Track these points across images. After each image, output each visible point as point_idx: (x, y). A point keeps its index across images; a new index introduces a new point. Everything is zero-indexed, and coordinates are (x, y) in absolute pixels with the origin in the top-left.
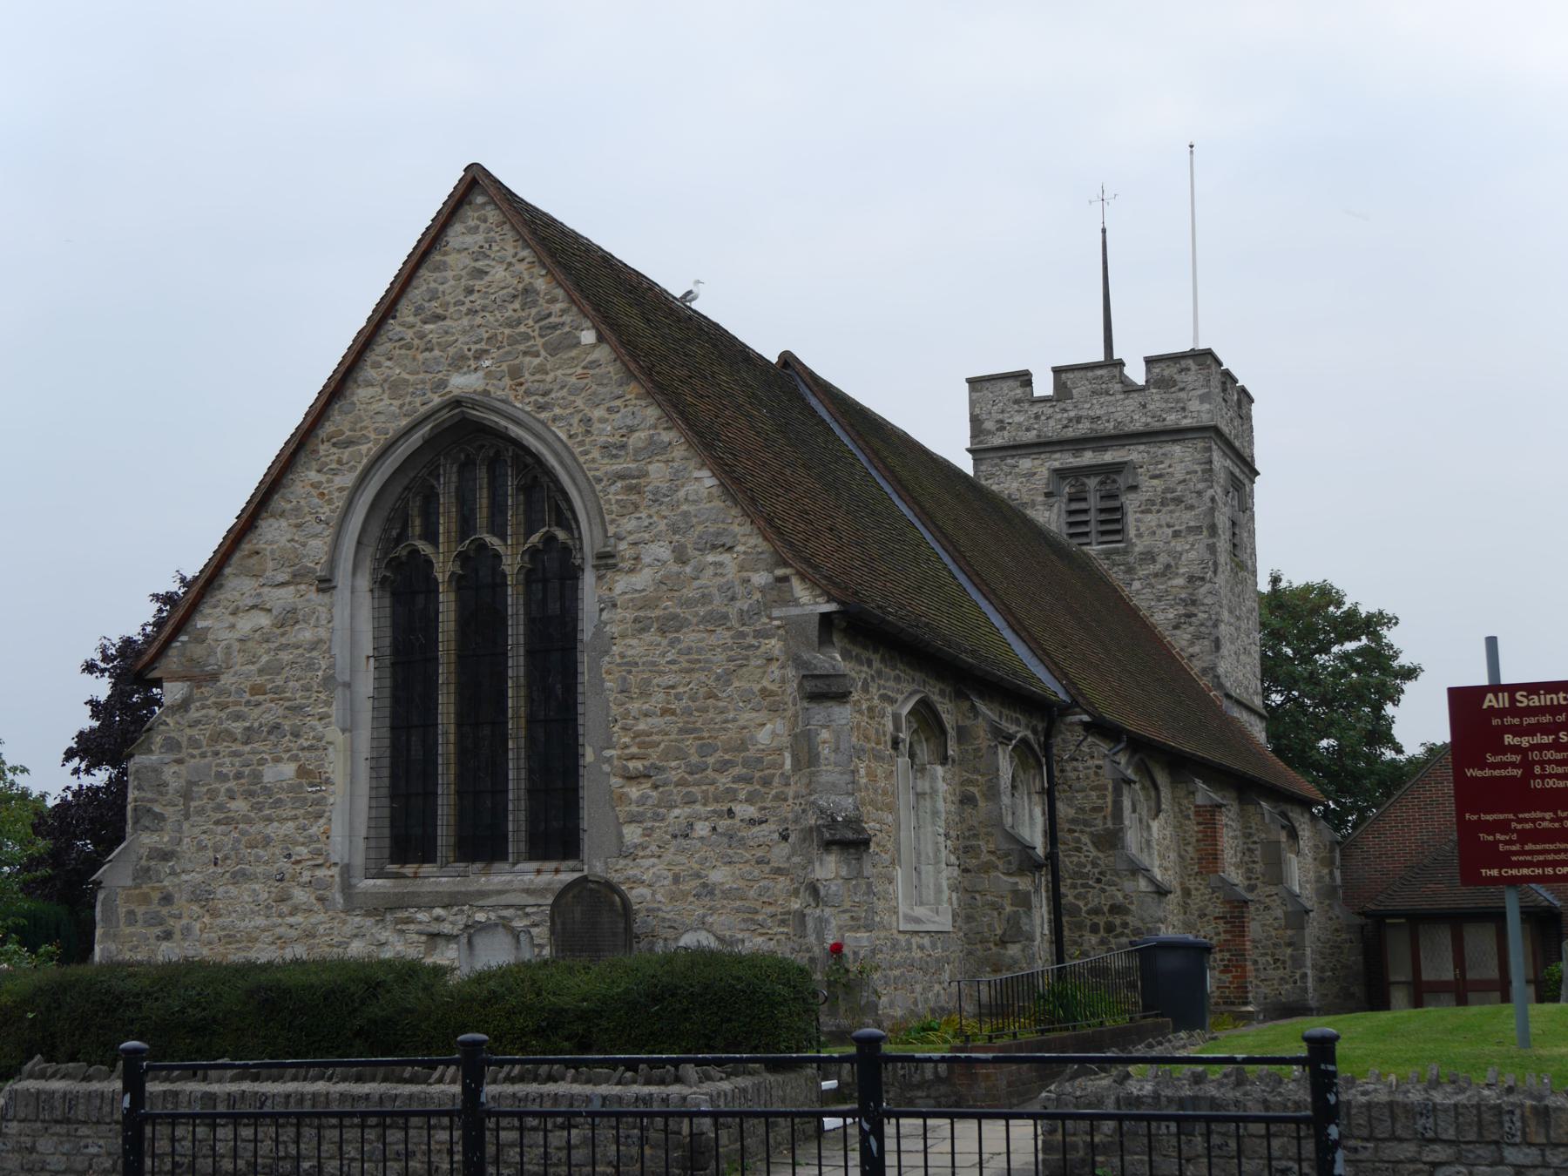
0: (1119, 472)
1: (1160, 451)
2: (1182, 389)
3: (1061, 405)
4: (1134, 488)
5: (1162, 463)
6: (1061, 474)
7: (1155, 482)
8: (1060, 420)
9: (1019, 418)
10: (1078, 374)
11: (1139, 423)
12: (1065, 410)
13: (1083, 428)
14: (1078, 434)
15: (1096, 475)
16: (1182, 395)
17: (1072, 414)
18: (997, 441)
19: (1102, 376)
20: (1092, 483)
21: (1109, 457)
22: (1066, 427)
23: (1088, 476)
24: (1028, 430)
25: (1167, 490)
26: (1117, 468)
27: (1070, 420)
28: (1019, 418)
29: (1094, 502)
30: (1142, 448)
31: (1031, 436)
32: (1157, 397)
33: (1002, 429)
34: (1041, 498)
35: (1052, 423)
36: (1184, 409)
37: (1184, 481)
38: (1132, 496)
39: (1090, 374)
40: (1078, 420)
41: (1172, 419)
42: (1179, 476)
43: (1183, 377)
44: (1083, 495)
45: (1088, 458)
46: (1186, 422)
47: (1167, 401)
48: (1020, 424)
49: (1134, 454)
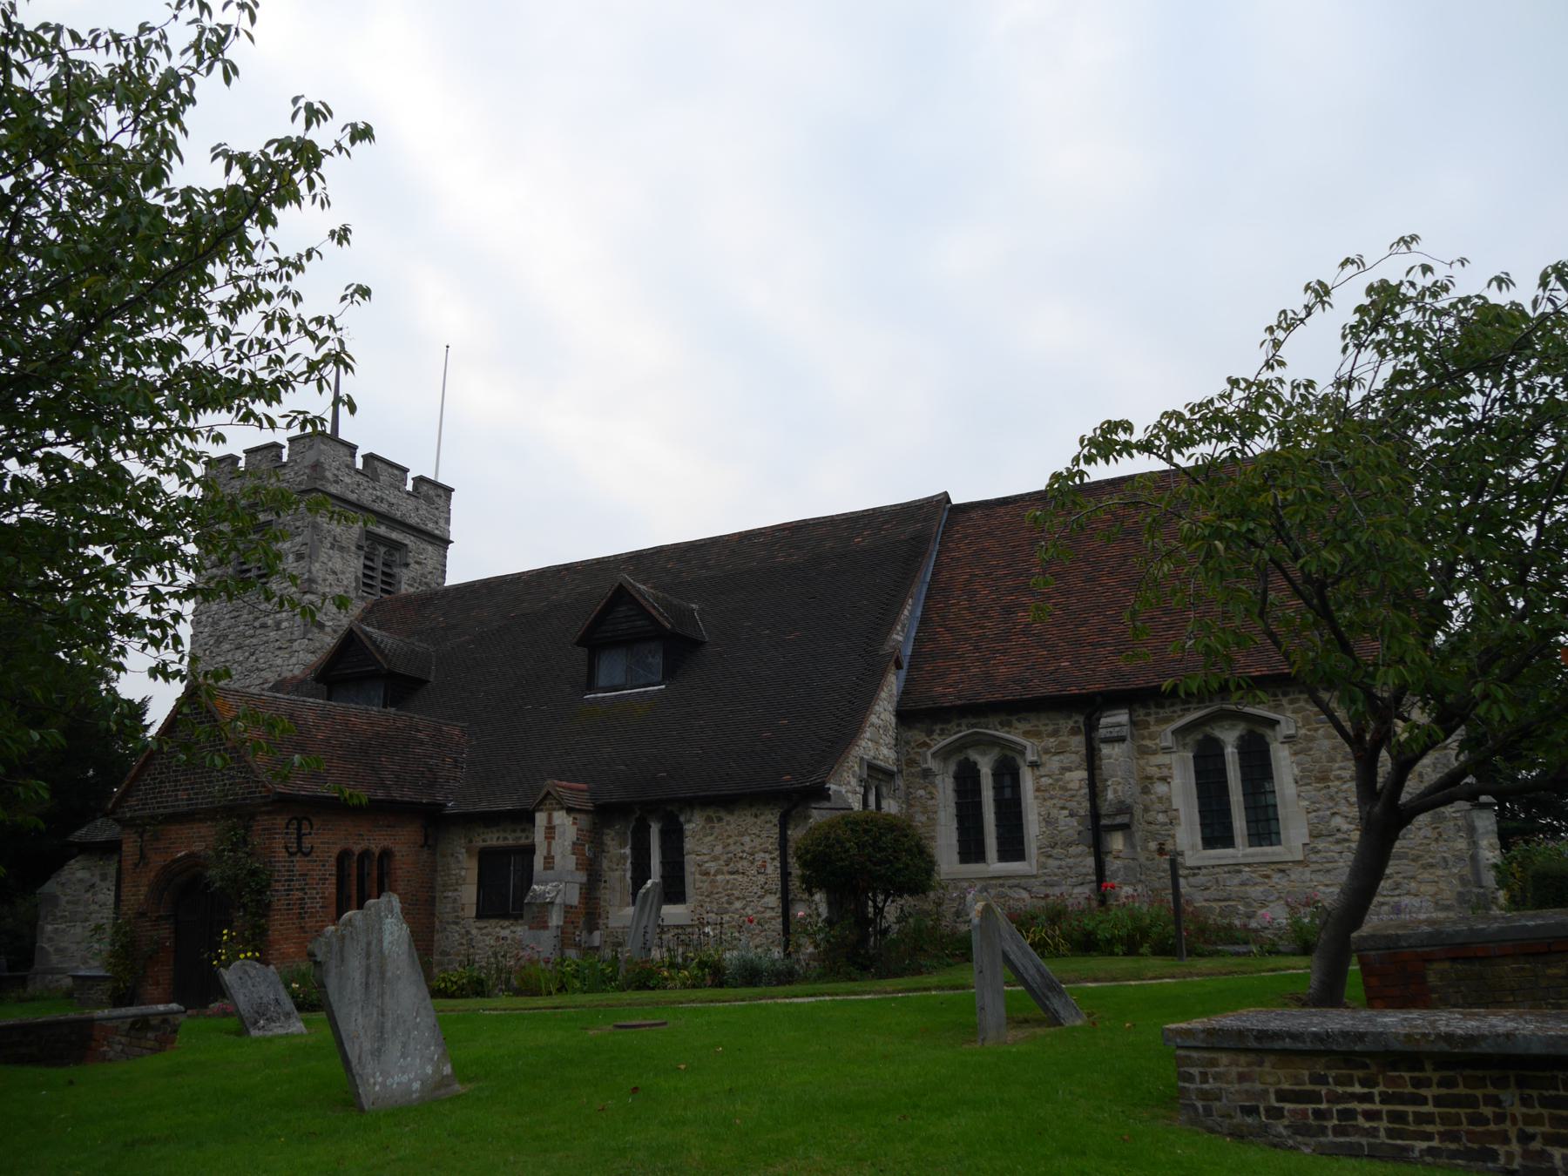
0: (397, 550)
1: (422, 546)
2: (437, 509)
3: (372, 484)
4: (407, 565)
5: (421, 554)
6: (370, 535)
7: (417, 566)
8: (371, 494)
9: (347, 480)
10: (385, 467)
11: (414, 520)
12: (374, 489)
13: (383, 508)
14: (381, 510)
15: (385, 546)
16: (436, 512)
17: (379, 493)
18: (333, 489)
19: (396, 476)
20: (382, 550)
21: (394, 535)
22: (374, 501)
23: (380, 544)
24: (352, 492)
25: (423, 575)
26: (397, 546)
27: (377, 497)
28: (347, 480)
29: (378, 564)
30: (412, 538)
31: (353, 497)
32: (424, 507)
33: (336, 482)
34: (353, 548)
35: (366, 494)
36: (437, 523)
37: (431, 573)
38: (404, 570)
39: (390, 470)
40: (382, 500)
41: (430, 526)
42: (429, 568)
43: (436, 499)
44: (372, 557)
45: (382, 530)
46: (437, 532)
47: (429, 512)
48: (347, 484)
49: (408, 540)
